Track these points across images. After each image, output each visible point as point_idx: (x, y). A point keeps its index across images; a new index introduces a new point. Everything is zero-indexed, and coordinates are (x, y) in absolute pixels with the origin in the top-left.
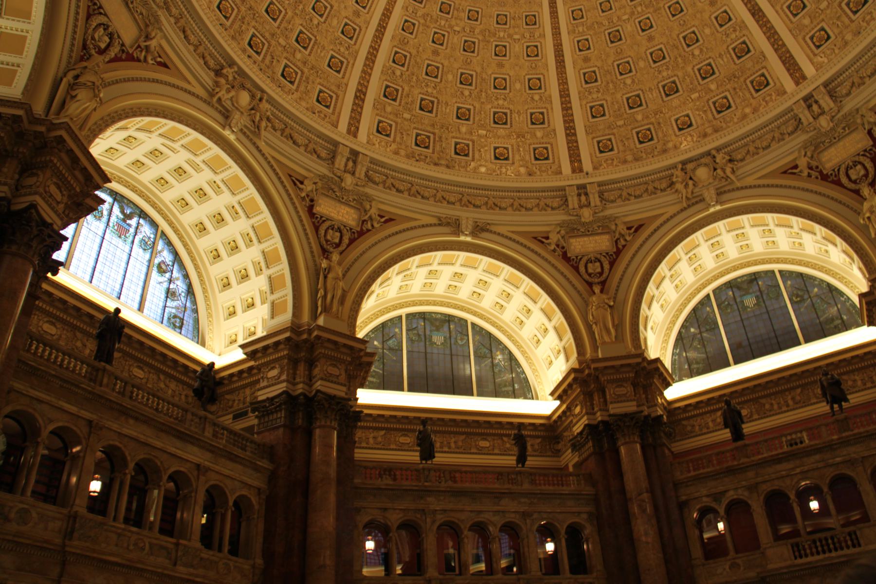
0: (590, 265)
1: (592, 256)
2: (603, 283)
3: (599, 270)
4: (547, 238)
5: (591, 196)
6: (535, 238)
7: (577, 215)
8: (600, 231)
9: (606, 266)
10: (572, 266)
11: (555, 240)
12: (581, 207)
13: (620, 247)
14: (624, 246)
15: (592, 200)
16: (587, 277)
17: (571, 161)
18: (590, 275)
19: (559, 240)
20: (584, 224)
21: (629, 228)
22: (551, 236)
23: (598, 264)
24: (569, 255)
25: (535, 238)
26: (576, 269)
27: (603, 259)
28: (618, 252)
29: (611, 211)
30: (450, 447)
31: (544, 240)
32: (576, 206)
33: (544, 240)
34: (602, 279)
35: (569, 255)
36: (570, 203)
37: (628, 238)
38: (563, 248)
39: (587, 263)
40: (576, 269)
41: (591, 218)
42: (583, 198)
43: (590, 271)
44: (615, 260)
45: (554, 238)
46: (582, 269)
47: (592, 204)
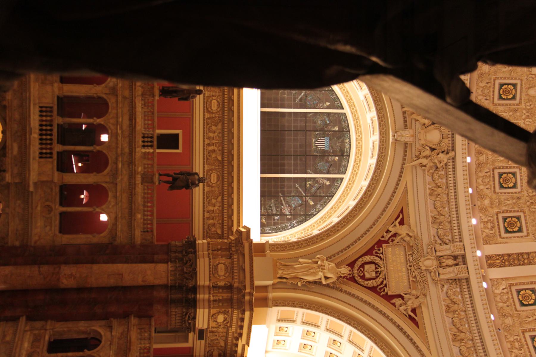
0: (373, 266)
1: (382, 268)
2: (352, 279)
3: (367, 275)
4: (402, 223)
5: (451, 269)
6: (402, 211)
7: (428, 253)
8: (411, 279)
9: (370, 283)
10: (372, 248)
11: (399, 232)
12: (439, 259)
13: (393, 301)
14: (394, 304)
15: (448, 270)
16: (359, 263)
17: (503, 255)
18: (362, 266)
19: (400, 235)
20: (418, 260)
21: (414, 311)
22: (404, 227)
23: (374, 275)
24: (383, 245)
25: (402, 211)
26: (369, 252)
27: (379, 280)
28: (388, 298)
29: (433, 289)
30: (209, 145)
31: (399, 220)
32: (439, 254)
33: (399, 220)
34: (357, 278)
35: (383, 245)
36: (445, 247)
37: (402, 308)
38: (393, 241)
39: (376, 264)
40: (369, 252)
41: (423, 268)
42: (451, 262)
43: (367, 267)
44: (379, 294)
45: (403, 230)
46: (368, 258)
47: (441, 270)
